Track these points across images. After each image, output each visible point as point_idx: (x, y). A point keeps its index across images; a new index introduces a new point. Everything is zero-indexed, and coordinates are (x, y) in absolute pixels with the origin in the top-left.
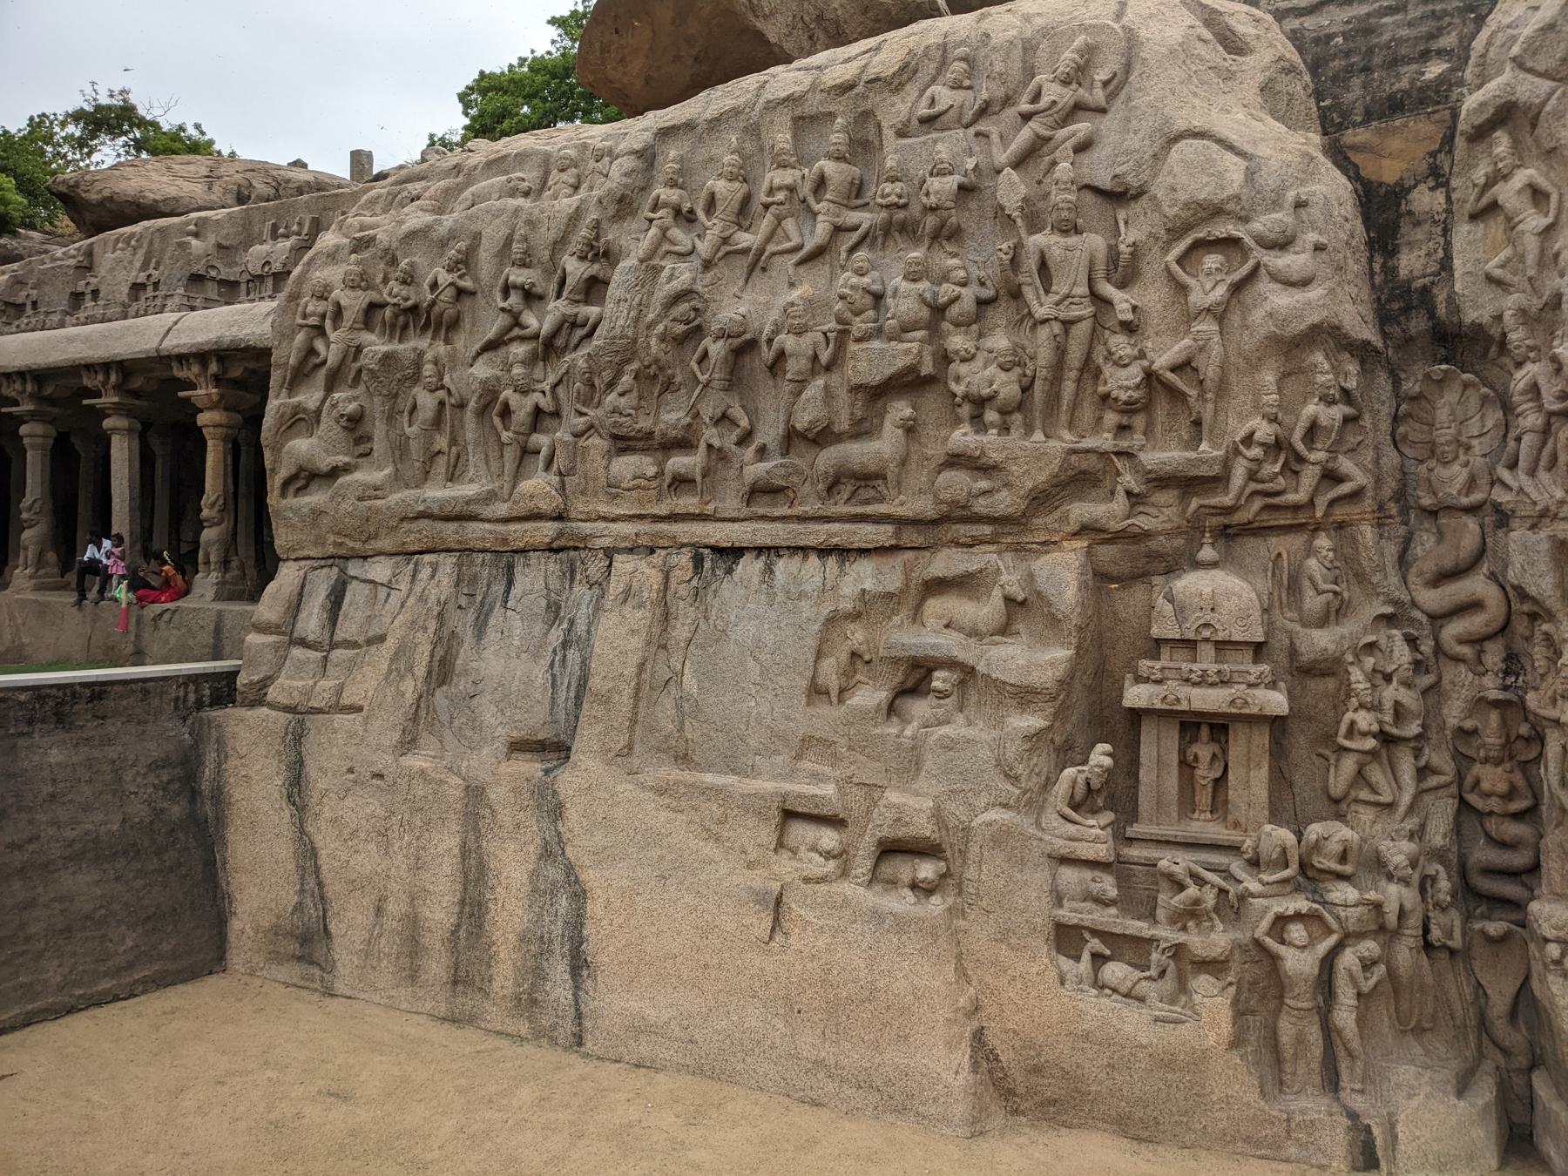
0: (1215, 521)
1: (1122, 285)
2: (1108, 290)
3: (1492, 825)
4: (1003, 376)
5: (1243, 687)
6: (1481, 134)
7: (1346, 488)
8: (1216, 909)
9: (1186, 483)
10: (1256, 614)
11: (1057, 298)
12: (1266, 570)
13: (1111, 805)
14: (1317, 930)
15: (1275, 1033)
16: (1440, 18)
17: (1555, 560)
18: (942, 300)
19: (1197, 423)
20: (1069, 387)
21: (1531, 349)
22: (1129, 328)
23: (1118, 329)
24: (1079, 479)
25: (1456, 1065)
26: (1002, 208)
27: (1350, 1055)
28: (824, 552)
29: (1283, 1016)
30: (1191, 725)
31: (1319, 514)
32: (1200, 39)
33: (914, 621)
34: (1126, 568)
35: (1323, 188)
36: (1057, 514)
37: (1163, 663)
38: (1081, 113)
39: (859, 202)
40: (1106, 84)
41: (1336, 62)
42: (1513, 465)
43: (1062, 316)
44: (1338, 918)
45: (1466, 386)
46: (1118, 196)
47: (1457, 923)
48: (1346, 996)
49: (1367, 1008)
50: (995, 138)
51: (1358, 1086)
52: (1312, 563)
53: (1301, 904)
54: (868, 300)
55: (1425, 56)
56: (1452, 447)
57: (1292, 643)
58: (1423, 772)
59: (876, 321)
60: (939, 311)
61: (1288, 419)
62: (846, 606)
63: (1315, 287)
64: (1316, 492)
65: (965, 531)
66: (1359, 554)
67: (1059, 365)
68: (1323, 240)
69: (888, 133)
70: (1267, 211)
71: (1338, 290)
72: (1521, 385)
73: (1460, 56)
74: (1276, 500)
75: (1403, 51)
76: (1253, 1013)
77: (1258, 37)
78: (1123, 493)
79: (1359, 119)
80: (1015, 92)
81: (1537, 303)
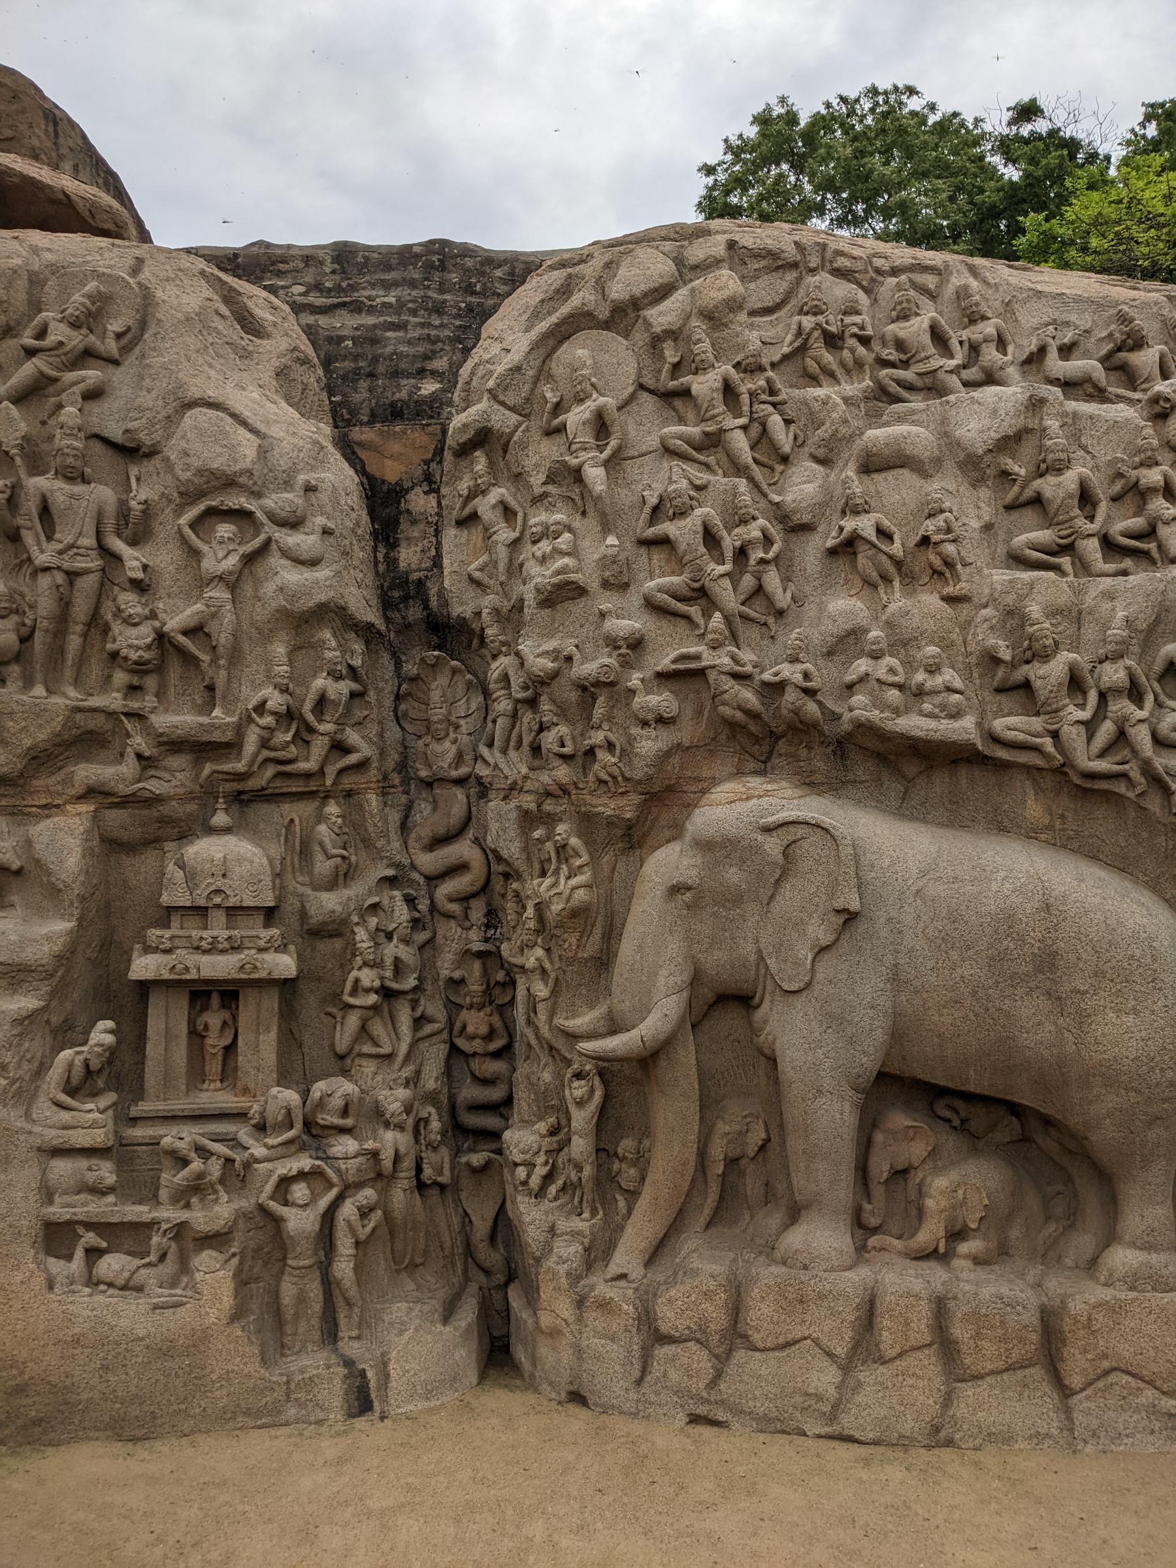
1: (133, 542)
2: (118, 545)
3: (475, 1064)
5: (253, 951)
6: (464, 451)
7: (353, 759)
8: (222, 1181)
9: (201, 748)
10: (267, 880)
13: (116, 1083)
14: (319, 1185)
15: (277, 1296)
16: (434, 343)
17: (520, 827)
19: (211, 688)
20: (74, 642)
21: (503, 644)
23: (128, 586)
24: (86, 738)
25: (443, 1293)
27: (348, 1304)
29: (286, 1277)
30: (201, 993)
31: (328, 782)
34: (137, 833)
35: (332, 477)
36: (60, 776)
37: (174, 931)
38: (92, 361)
40: (119, 336)
41: (346, 363)
42: (490, 745)
44: (338, 1171)
45: (454, 671)
46: (130, 451)
47: (447, 1160)
48: (345, 1246)
49: (365, 1255)
51: (354, 1333)
52: (322, 828)
53: (305, 1162)
55: (421, 373)
56: (444, 726)
57: (303, 907)
58: (419, 1022)
61: (298, 691)
63: (322, 567)
66: (365, 819)
68: (331, 525)
71: (345, 573)
72: (496, 675)
73: (449, 378)
74: (288, 768)
75: (403, 365)
76: (257, 1280)
77: (275, 324)
78: (133, 756)
79: (365, 419)
80: (19, 324)
81: (507, 605)
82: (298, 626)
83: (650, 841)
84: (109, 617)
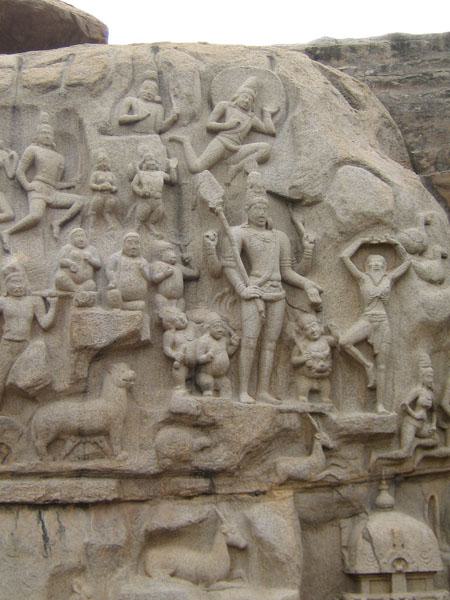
0: (388, 471)
1: (304, 274)
2: (295, 276)
4: (215, 343)
9: (369, 439)
11: (259, 280)
12: (423, 509)
18: (159, 275)
19: (373, 389)
20: (268, 356)
22: (316, 308)
23: (307, 308)
26: (204, 202)
28: (39, 506)
32: (333, 93)
33: (137, 572)
36: (264, 467)
38: (254, 135)
39: (65, 184)
40: (273, 115)
43: (266, 295)
50: (188, 145)
54: (89, 270)
59: (96, 289)
60: (154, 285)
62: (72, 560)
65: (187, 484)
67: (261, 339)
69: (91, 132)
70: (406, 226)
78: (320, 448)
84: (294, 334)
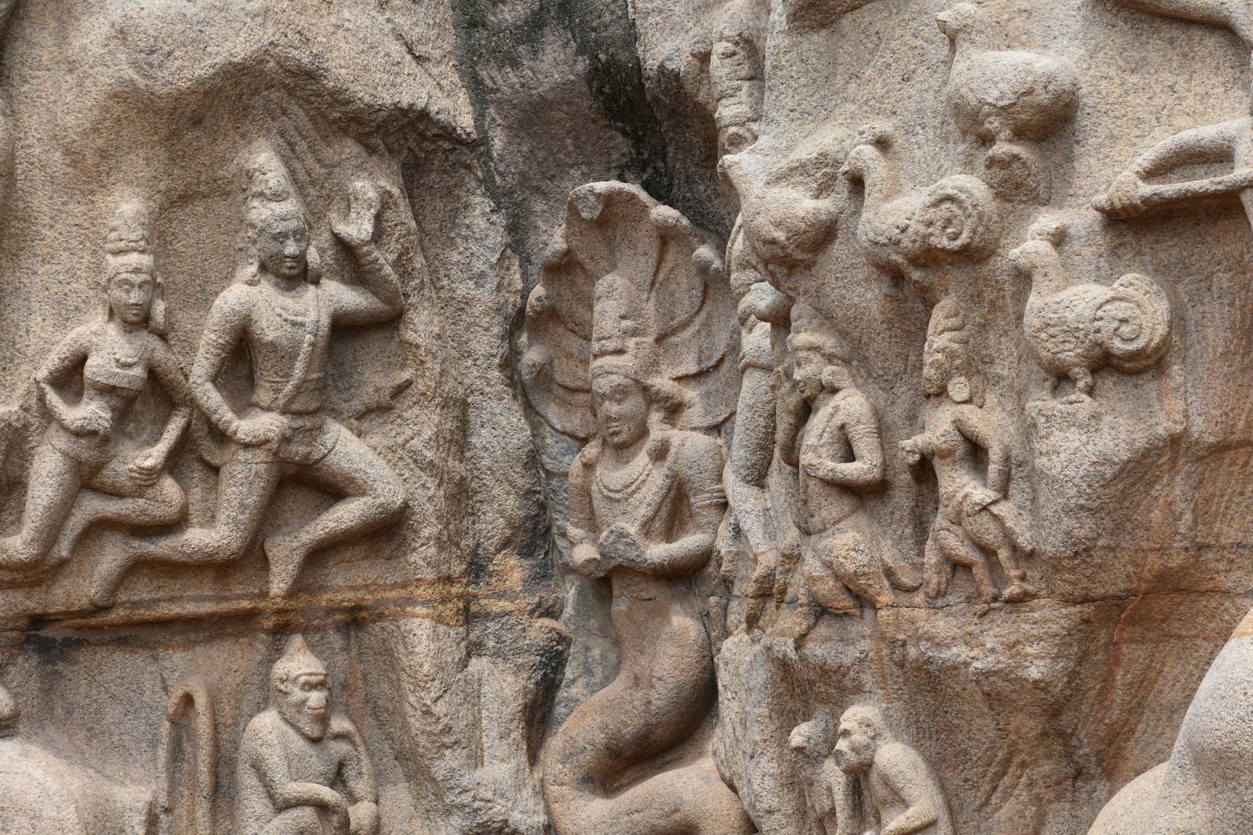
31: (278, 584)
45: (666, 237)
52: (267, 723)
61: (184, 320)
64: (267, 519)
74: (162, 547)
82: (173, 137)
83: (1133, 751)
